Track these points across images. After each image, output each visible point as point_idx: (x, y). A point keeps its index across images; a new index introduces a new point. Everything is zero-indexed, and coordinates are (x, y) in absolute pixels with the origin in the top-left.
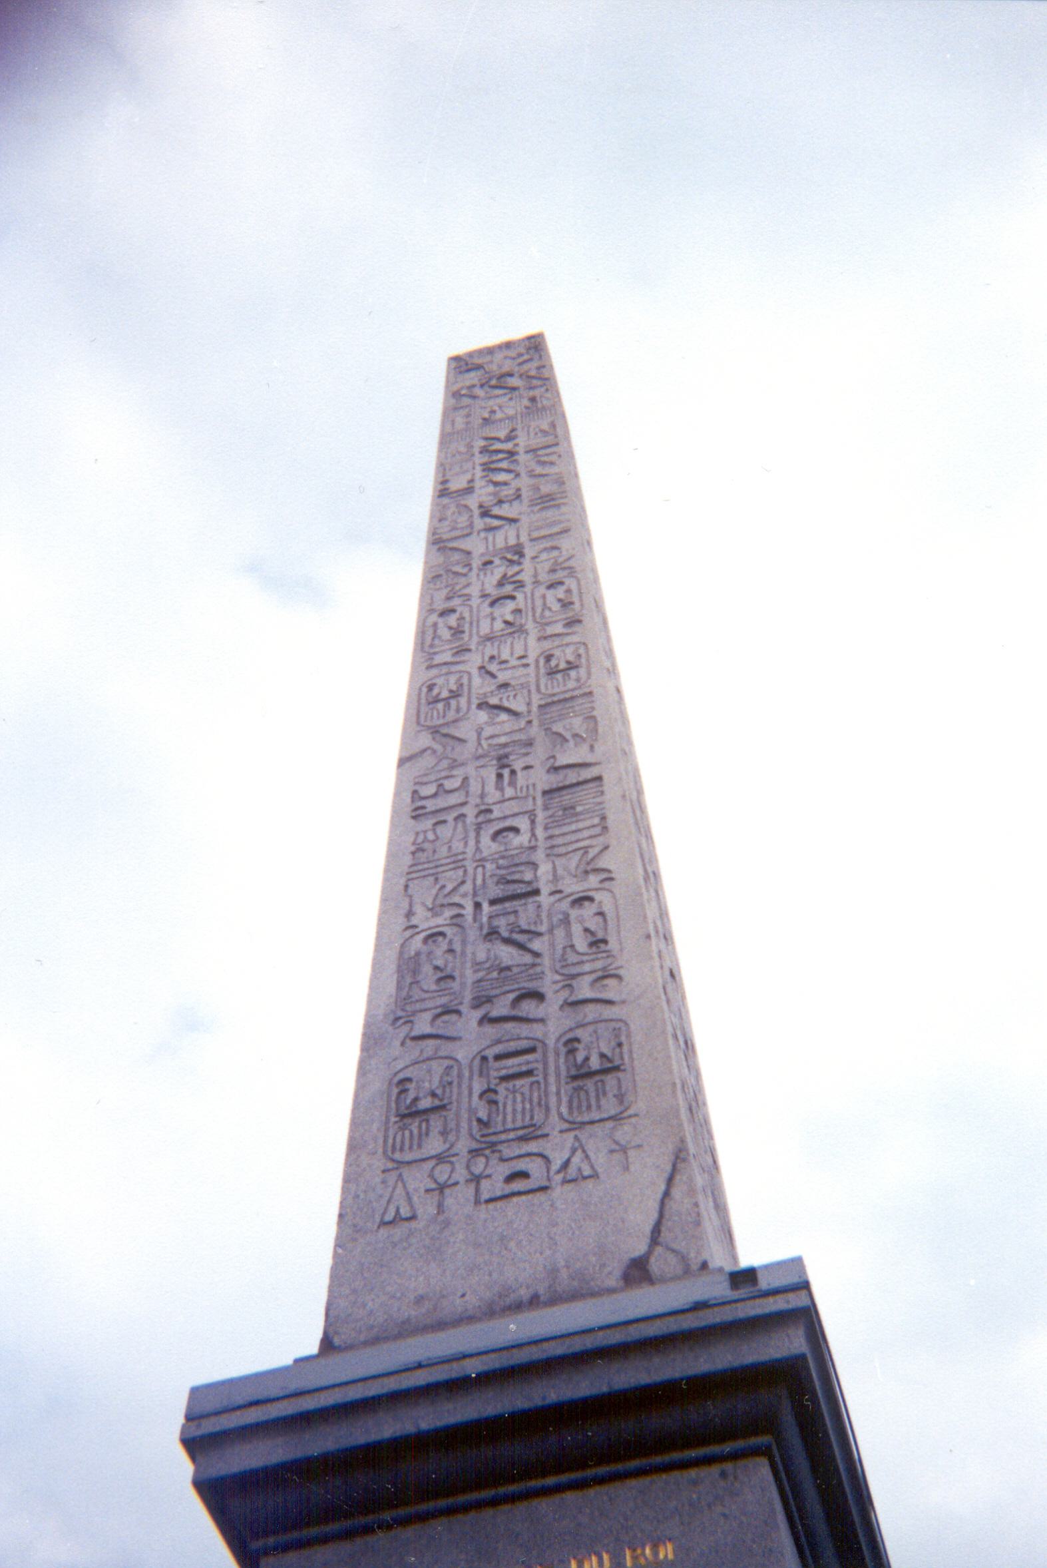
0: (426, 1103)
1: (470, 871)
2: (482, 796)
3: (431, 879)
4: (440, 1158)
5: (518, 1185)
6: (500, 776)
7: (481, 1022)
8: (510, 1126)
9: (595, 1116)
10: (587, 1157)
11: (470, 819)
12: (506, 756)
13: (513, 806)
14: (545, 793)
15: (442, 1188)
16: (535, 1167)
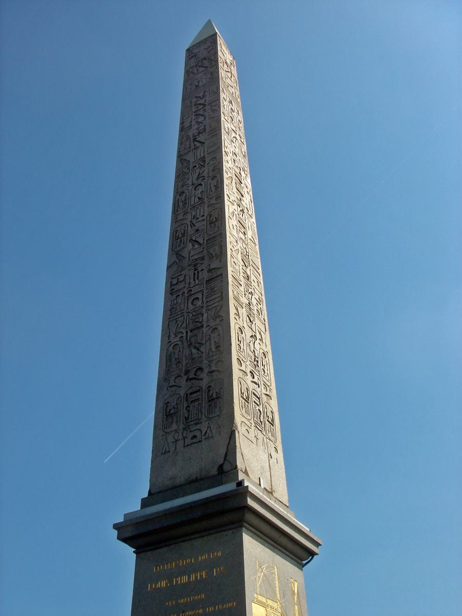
0: (172, 411)
1: (185, 317)
2: (189, 284)
3: (175, 321)
4: (176, 431)
5: (194, 441)
6: (194, 274)
7: (187, 381)
8: (193, 419)
9: (213, 415)
10: (211, 430)
11: (186, 295)
12: (197, 264)
13: (197, 289)
14: (207, 281)
15: (177, 441)
16: (198, 434)
